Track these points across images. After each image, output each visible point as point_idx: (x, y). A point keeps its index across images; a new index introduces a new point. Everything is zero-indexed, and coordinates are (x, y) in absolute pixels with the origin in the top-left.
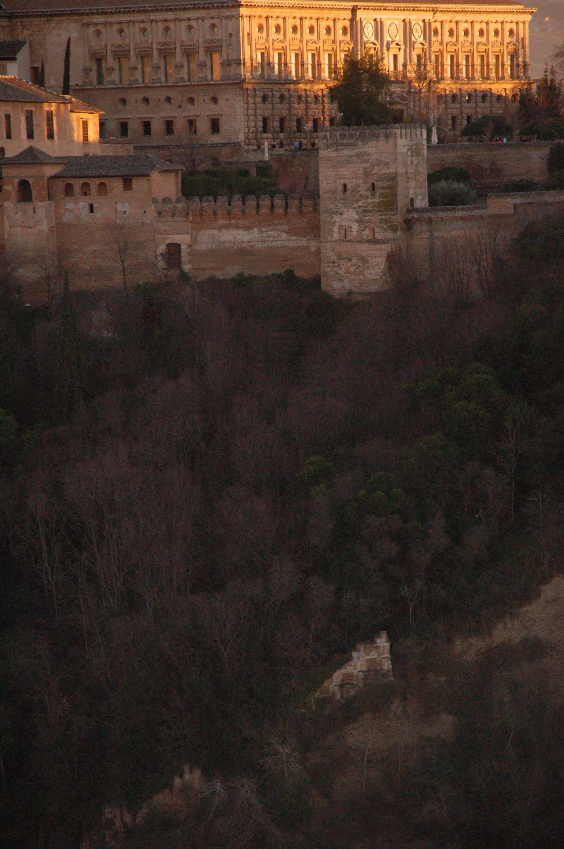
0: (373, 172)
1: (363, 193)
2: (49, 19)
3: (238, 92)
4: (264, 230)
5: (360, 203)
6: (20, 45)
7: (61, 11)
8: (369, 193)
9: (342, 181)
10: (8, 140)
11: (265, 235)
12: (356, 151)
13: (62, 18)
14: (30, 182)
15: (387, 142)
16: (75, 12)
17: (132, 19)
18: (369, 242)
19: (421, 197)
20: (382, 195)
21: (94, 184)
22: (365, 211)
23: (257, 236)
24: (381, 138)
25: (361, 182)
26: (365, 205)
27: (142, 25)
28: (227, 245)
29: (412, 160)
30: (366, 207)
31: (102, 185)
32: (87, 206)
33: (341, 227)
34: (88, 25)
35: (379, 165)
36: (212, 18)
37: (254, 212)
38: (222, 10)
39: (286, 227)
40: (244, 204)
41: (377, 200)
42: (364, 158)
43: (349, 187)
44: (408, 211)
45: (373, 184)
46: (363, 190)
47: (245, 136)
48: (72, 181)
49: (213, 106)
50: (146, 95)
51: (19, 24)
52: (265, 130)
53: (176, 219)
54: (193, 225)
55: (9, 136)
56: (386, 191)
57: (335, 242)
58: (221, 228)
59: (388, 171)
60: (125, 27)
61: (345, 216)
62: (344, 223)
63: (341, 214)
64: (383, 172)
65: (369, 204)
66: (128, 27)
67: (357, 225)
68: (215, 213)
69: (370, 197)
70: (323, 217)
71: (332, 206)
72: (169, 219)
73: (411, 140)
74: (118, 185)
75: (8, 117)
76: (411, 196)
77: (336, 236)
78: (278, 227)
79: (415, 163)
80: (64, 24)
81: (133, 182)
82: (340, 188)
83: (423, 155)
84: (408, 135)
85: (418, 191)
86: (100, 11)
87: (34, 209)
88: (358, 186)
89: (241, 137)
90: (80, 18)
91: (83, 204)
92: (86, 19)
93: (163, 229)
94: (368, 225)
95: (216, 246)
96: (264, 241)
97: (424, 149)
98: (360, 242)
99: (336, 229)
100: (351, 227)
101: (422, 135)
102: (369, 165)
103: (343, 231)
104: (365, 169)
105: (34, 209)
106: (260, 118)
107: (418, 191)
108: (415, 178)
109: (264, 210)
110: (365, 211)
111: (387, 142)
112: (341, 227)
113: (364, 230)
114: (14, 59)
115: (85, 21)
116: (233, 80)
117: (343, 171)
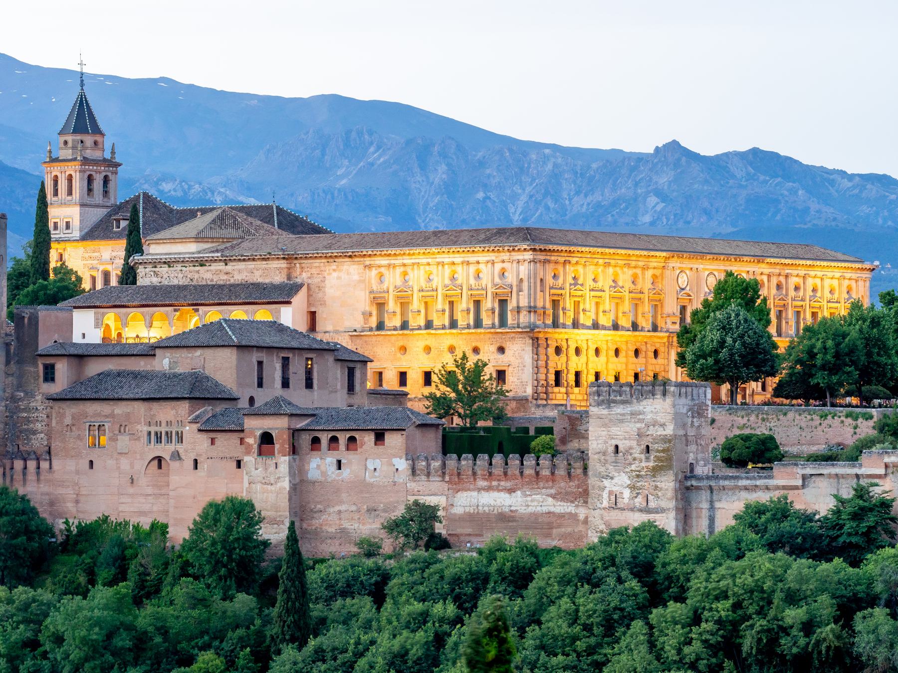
0: (649, 433)
1: (636, 455)
2: (329, 260)
3: (527, 341)
4: (527, 493)
5: (633, 467)
6: (296, 288)
7: (342, 253)
8: (643, 456)
9: (614, 442)
10: (260, 389)
11: (529, 499)
12: (629, 409)
13: (343, 260)
14: (274, 435)
15: (665, 400)
16: (357, 254)
17: (417, 261)
18: (641, 510)
19: (702, 462)
20: (658, 459)
21: (343, 438)
22: (638, 476)
23: (520, 500)
24: (658, 396)
25: (634, 443)
26: (637, 469)
27: (427, 268)
28: (486, 509)
29: (692, 422)
30: (639, 471)
31: (352, 439)
32: (335, 462)
33: (611, 493)
34: (369, 267)
35: (654, 426)
36: (503, 262)
37: (517, 472)
38: (513, 253)
39: (553, 491)
40: (522, 464)
41: (651, 464)
42: (638, 417)
43: (621, 448)
44: (686, 478)
45: (648, 447)
46: (637, 452)
47: (533, 389)
48: (338, 435)
49: (500, 356)
50: (428, 343)
51: (298, 265)
52: (558, 383)
53: (432, 479)
54: (450, 486)
55: (260, 385)
56: (662, 454)
57: (604, 509)
58: (479, 490)
59: (664, 433)
60: (409, 269)
61: (615, 480)
62: (614, 489)
63: (612, 478)
64: (659, 433)
65: (643, 468)
66: (413, 269)
67: (629, 491)
68: (474, 474)
69: (644, 460)
70: (592, 481)
71: (602, 469)
72: (424, 478)
73: (693, 399)
74: (369, 439)
75: (260, 363)
76: (691, 461)
77: (605, 504)
78: (544, 491)
79: (696, 424)
80: (345, 267)
81: (386, 437)
82: (611, 449)
83: (707, 417)
84: (689, 394)
85: (700, 456)
86: (383, 253)
87: (276, 464)
88: (631, 448)
89: (529, 391)
90: (362, 259)
91: (331, 460)
92: (368, 261)
93: (416, 490)
94: (641, 491)
95: (474, 510)
96: (528, 506)
97: (707, 410)
98: (632, 510)
99: (605, 495)
100: (622, 493)
101: (705, 395)
102: (643, 425)
103: (613, 498)
104: (639, 429)
105: (276, 464)
106: (552, 371)
107: (700, 456)
108: (696, 441)
109: (529, 472)
110: (638, 476)
111: (665, 400)
112: (611, 493)
113: (636, 497)
114: (289, 303)
115: (367, 263)
116: (522, 328)
117: (615, 430)
